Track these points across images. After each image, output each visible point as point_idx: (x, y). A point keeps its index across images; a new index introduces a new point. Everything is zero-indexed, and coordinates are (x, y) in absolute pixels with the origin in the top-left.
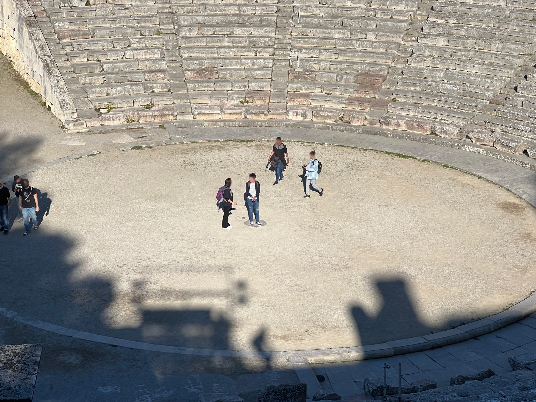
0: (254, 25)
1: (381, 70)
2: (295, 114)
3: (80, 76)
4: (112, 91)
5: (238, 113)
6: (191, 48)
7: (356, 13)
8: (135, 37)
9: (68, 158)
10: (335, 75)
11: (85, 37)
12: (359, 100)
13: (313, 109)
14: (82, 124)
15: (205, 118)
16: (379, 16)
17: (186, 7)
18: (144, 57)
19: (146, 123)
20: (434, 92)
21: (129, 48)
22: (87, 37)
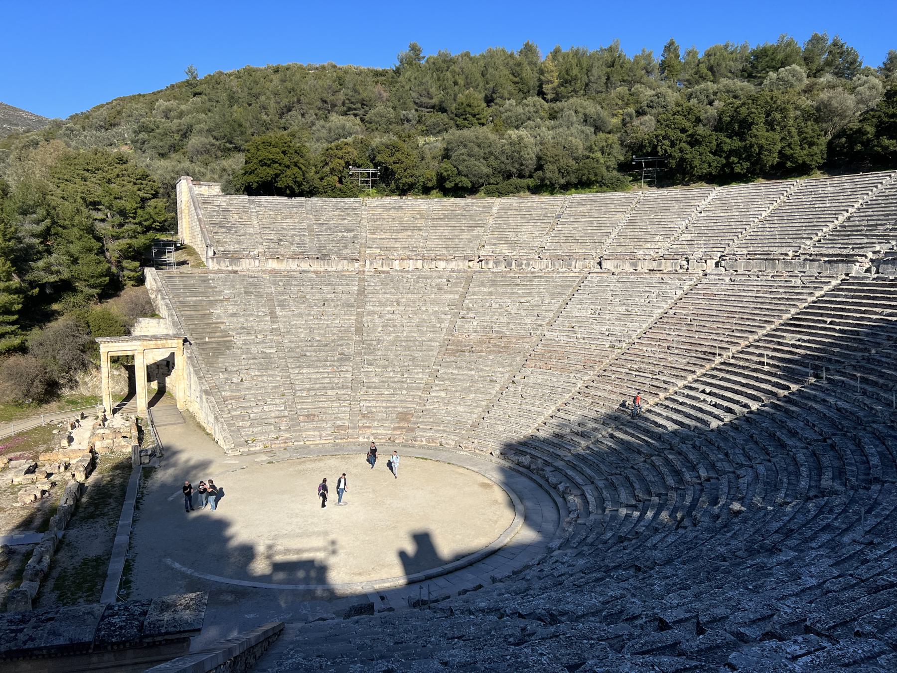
0: (339, 388)
4: (255, 430)
7: (396, 379)
9: (228, 471)
12: (399, 428)
13: (373, 434)
15: (311, 443)
16: (408, 381)
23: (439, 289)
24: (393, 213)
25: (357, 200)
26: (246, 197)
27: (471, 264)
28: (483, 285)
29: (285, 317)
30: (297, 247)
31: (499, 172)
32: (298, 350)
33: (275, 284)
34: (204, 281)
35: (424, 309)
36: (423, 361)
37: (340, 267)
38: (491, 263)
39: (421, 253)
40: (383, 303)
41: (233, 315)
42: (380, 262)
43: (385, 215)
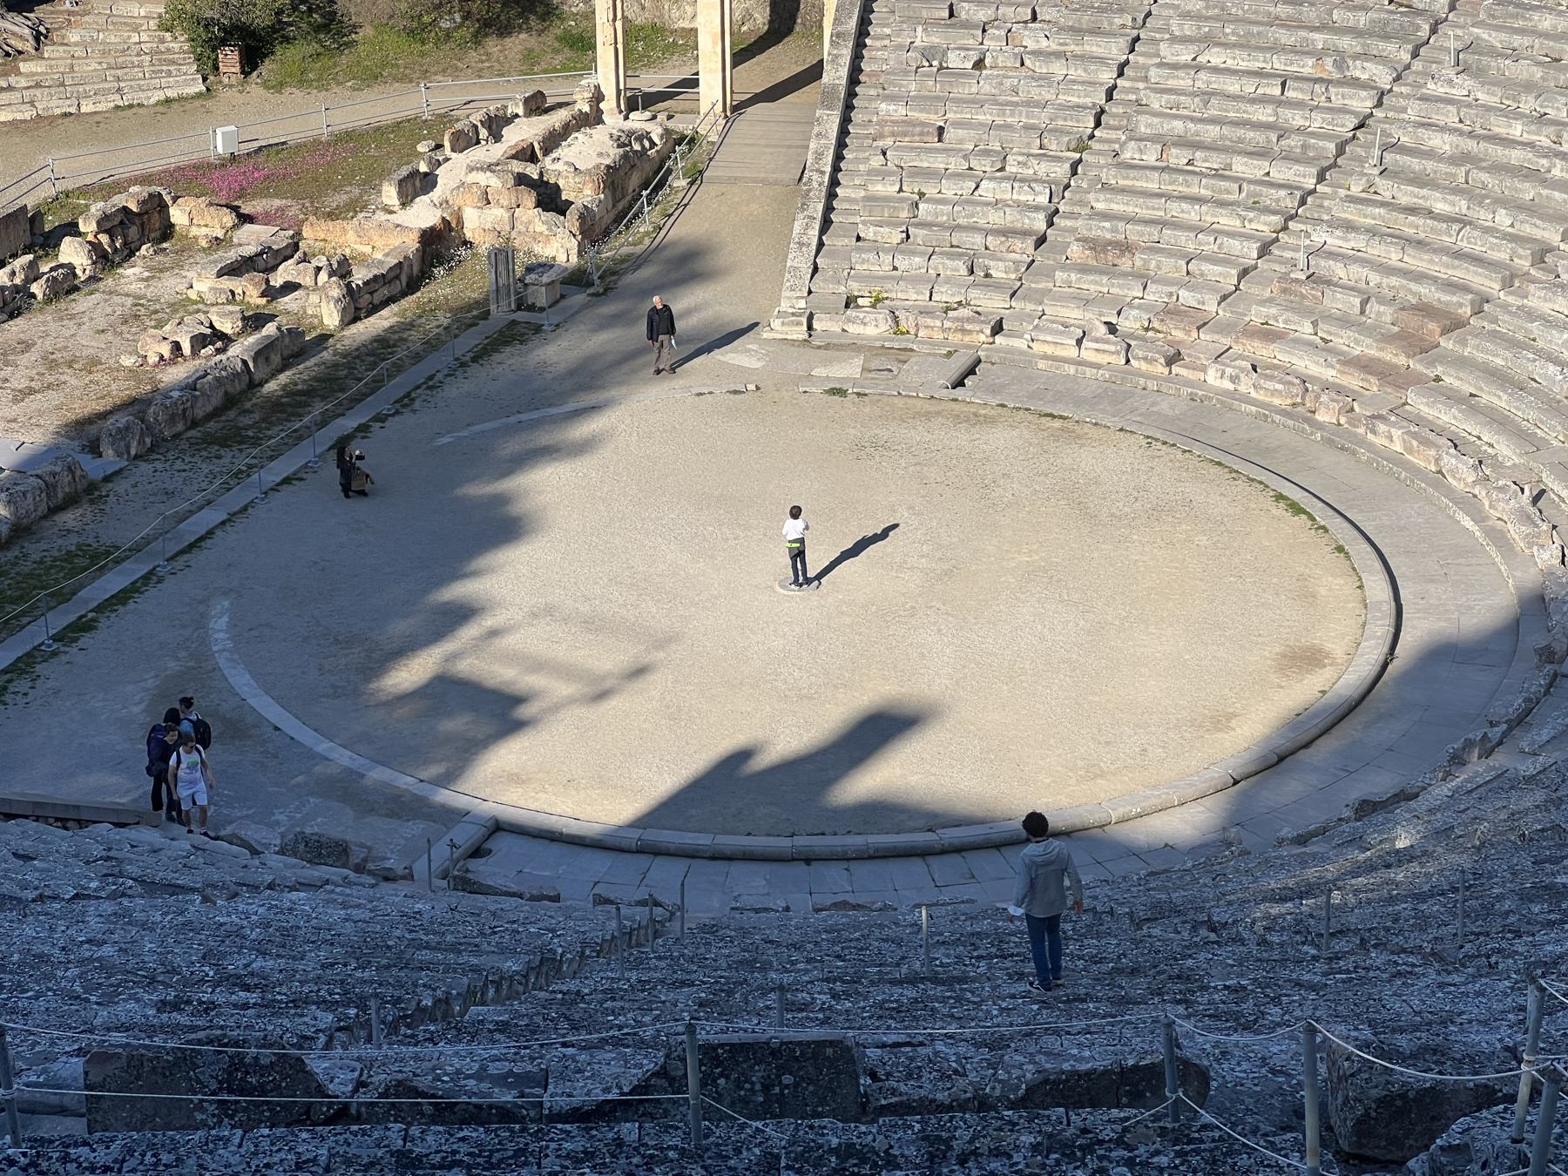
0: (1288, 157)
1: (1461, 305)
2: (1219, 375)
3: (864, 223)
5: (1113, 353)
6: (1123, 191)
7: (1516, 156)
8: (1025, 151)
10: (1357, 301)
12: (1365, 366)
14: (799, 324)
15: (1049, 350)
17: (1165, 96)
18: (1015, 197)
19: (930, 341)
20: (1524, 377)
21: (998, 174)
22: (929, 139)
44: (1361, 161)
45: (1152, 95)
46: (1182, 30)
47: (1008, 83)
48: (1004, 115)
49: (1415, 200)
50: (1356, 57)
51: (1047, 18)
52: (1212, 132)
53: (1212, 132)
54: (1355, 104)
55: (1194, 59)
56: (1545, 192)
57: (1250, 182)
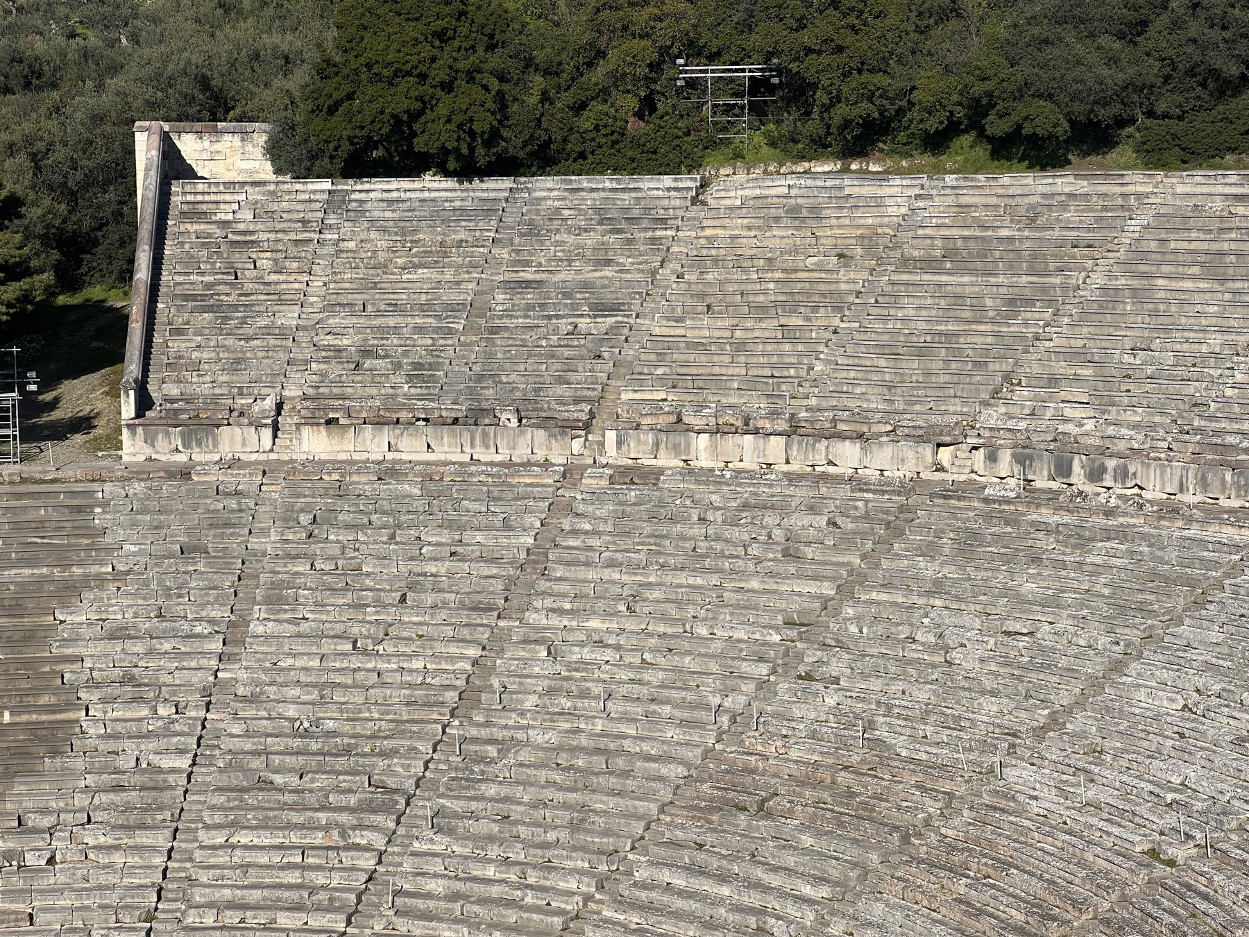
0: (319, 908)
7: (495, 891)
8: (104, 926)
11: (19, 924)
16: (529, 900)
17: (212, 871)
22: (22, 924)
23: (789, 554)
24: (780, 237)
25: (689, 182)
26: (326, 184)
27: (945, 454)
28: (929, 551)
29: (267, 638)
30: (410, 379)
31: (1191, 73)
32: (256, 763)
33: (288, 518)
34: (79, 509)
35: (703, 631)
36: (606, 833)
37: (521, 453)
38: (1006, 457)
39: (789, 406)
40: (582, 605)
41: (119, 634)
42: (650, 438)
43: (747, 246)
44: (377, 906)
45: (201, 871)
46: (213, 819)
47: (79, 873)
48: (81, 898)
49: (427, 931)
50: (354, 828)
51: (100, 819)
52: (256, 895)
53: (256, 895)
54: (361, 863)
55: (227, 841)
56: (525, 915)
57: (294, 931)
